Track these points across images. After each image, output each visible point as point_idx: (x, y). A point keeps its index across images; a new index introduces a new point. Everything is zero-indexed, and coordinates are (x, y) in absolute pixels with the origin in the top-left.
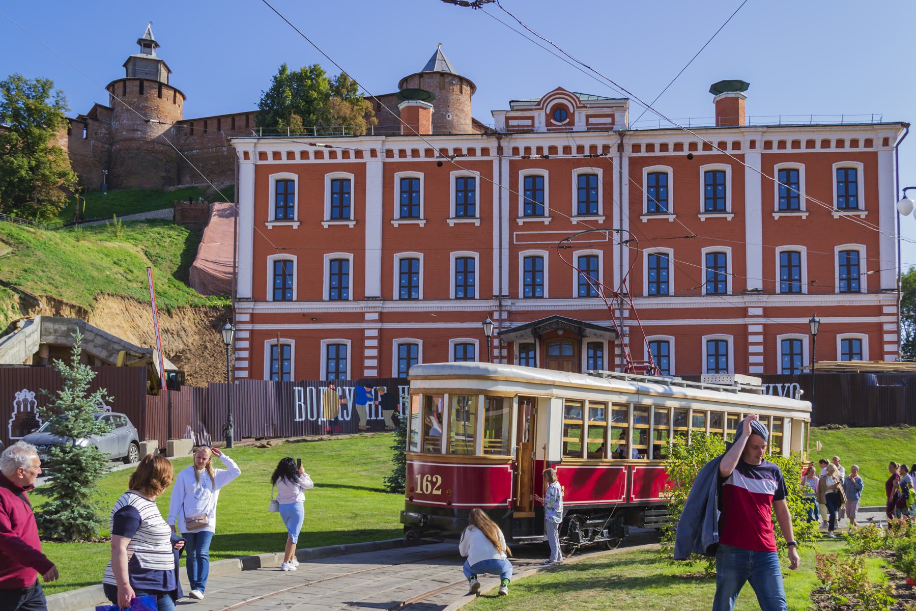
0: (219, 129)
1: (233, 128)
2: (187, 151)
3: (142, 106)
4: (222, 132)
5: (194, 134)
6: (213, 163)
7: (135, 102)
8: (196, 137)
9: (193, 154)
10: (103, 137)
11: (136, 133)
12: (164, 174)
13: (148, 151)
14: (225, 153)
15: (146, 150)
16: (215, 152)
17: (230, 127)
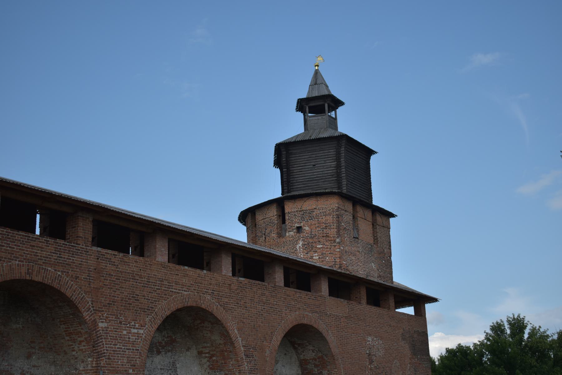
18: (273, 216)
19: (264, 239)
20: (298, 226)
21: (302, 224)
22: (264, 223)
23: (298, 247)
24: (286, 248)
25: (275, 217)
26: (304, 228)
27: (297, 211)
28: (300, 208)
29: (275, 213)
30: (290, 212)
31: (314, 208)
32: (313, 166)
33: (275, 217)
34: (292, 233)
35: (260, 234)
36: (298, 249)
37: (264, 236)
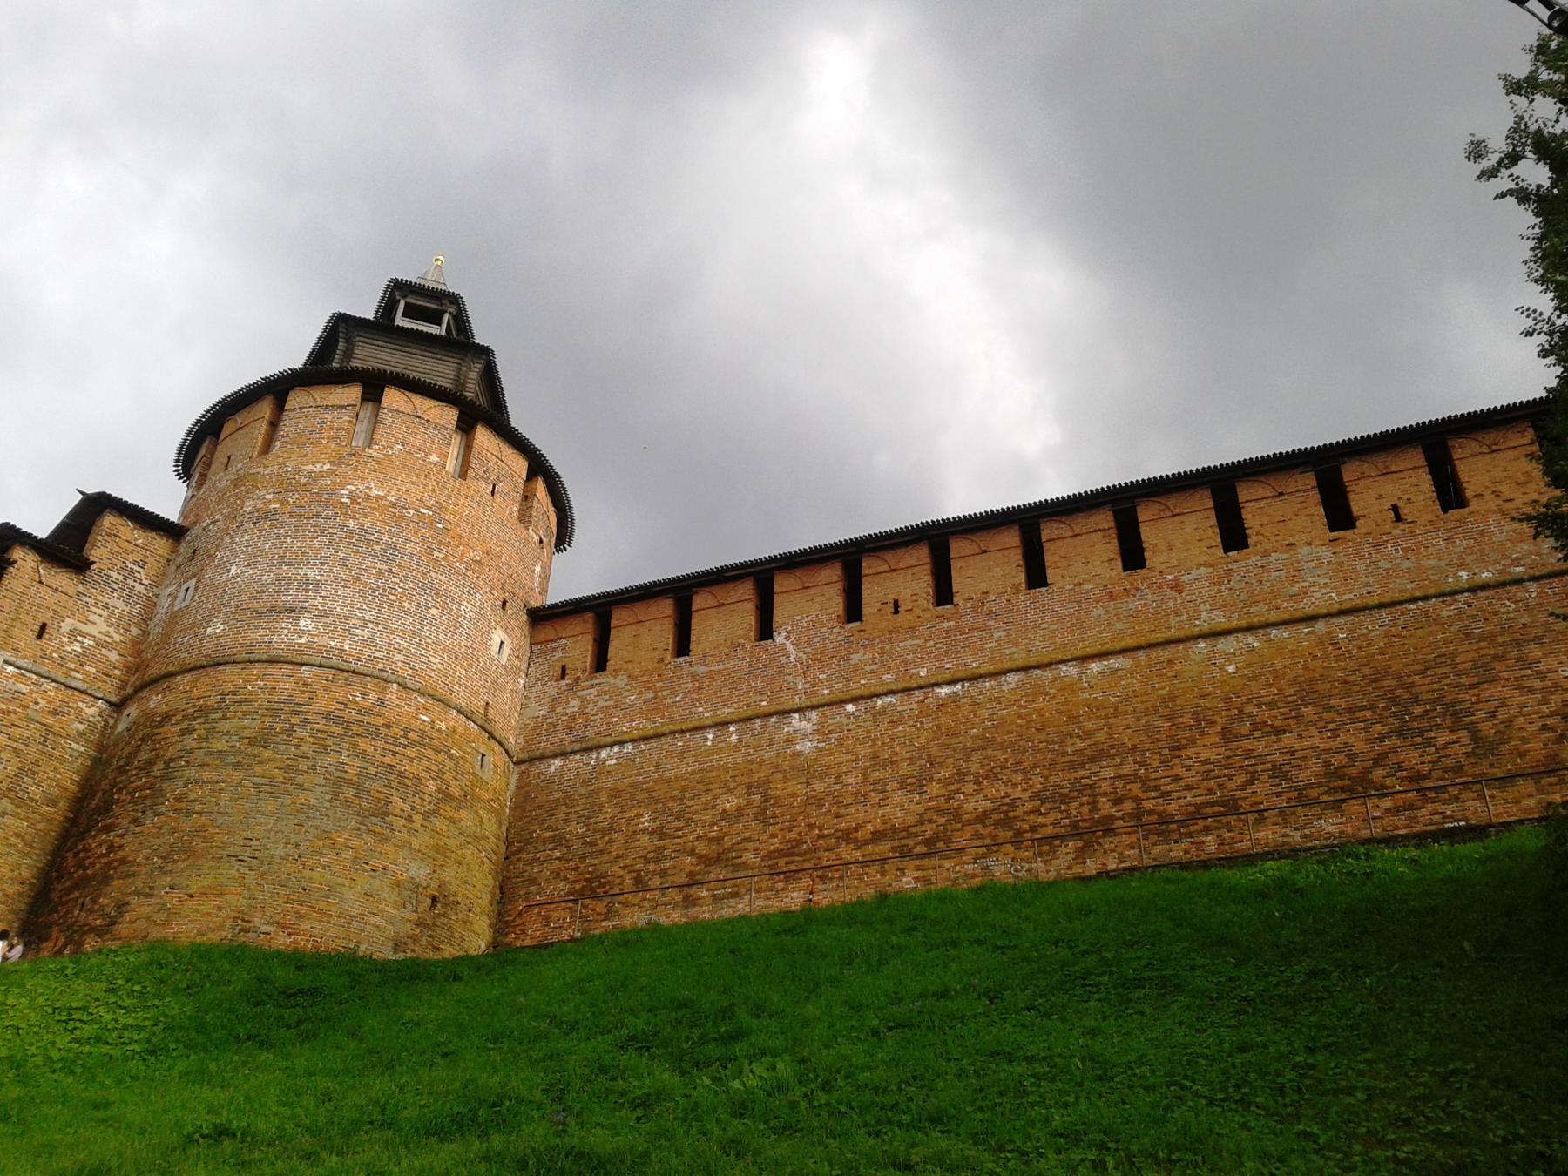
0: (765, 630)
1: (853, 612)
2: (564, 754)
3: (353, 500)
4: (780, 638)
5: (611, 665)
6: (731, 803)
7: (315, 478)
8: (621, 681)
9: (600, 768)
10: (82, 659)
11: (286, 623)
12: (419, 871)
13: (338, 721)
14: (805, 746)
15: (327, 716)
16: (736, 748)
17: (837, 605)
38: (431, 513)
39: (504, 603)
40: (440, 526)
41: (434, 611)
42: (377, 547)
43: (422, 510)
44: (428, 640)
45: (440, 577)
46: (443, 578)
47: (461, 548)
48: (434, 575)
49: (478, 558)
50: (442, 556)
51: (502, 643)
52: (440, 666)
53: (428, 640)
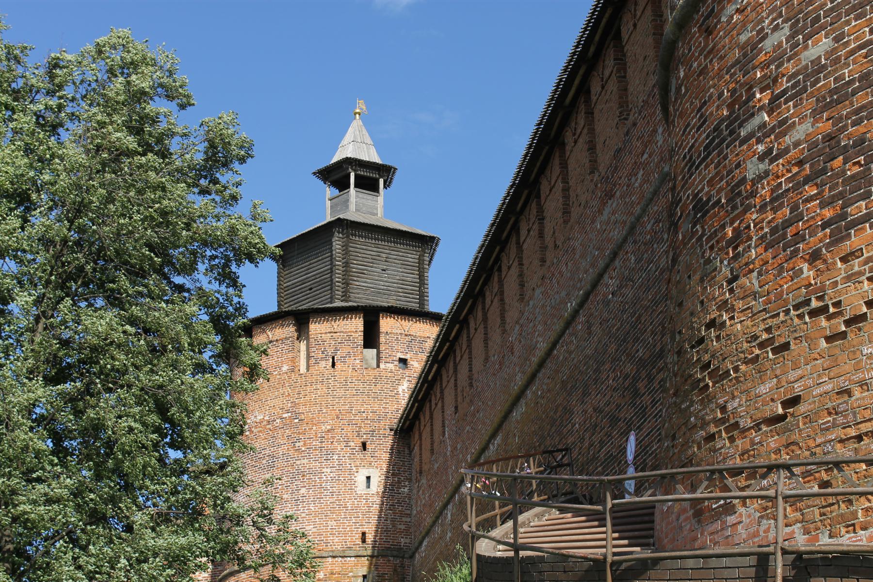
18: (356, 331)
19: (331, 364)
20: (401, 357)
21: (408, 357)
22: (332, 338)
23: (400, 390)
24: (379, 386)
25: (360, 334)
26: (412, 363)
27: (401, 334)
28: (406, 330)
29: (362, 328)
30: (390, 333)
31: (428, 337)
32: (383, 270)
33: (360, 334)
34: (390, 366)
35: (320, 355)
36: (400, 392)
37: (331, 360)
38: (290, 414)
39: (364, 445)
40: (297, 421)
41: (303, 491)
42: (264, 462)
43: (284, 416)
44: (303, 515)
45: (303, 461)
46: (306, 461)
47: (314, 428)
48: (298, 462)
49: (329, 427)
50: (302, 443)
51: (368, 478)
52: (314, 530)
53: (303, 515)
